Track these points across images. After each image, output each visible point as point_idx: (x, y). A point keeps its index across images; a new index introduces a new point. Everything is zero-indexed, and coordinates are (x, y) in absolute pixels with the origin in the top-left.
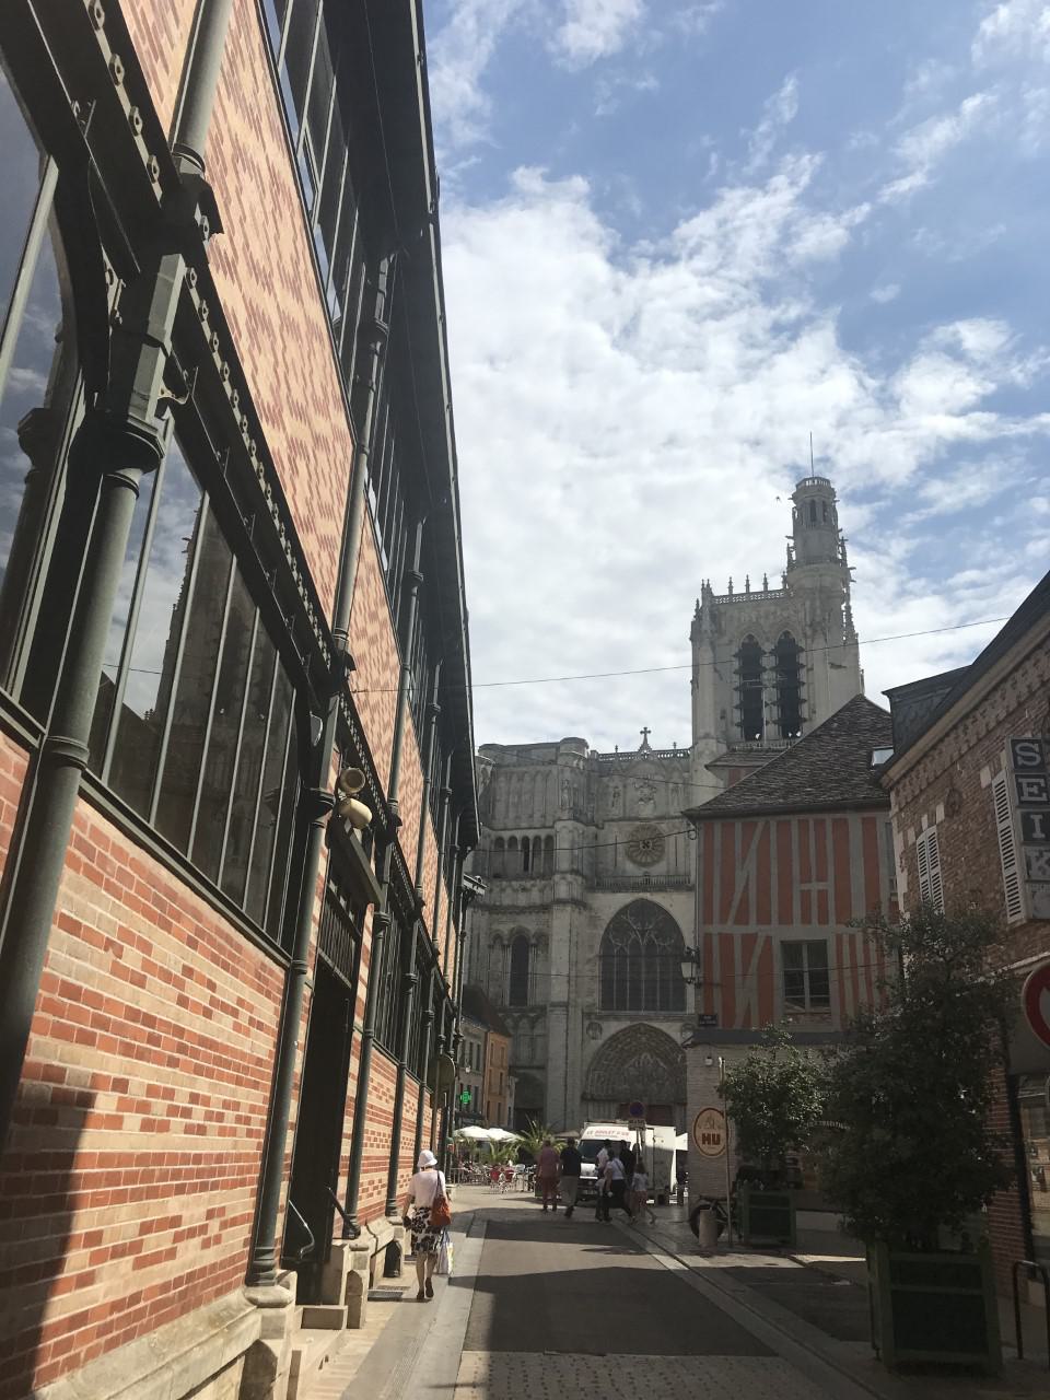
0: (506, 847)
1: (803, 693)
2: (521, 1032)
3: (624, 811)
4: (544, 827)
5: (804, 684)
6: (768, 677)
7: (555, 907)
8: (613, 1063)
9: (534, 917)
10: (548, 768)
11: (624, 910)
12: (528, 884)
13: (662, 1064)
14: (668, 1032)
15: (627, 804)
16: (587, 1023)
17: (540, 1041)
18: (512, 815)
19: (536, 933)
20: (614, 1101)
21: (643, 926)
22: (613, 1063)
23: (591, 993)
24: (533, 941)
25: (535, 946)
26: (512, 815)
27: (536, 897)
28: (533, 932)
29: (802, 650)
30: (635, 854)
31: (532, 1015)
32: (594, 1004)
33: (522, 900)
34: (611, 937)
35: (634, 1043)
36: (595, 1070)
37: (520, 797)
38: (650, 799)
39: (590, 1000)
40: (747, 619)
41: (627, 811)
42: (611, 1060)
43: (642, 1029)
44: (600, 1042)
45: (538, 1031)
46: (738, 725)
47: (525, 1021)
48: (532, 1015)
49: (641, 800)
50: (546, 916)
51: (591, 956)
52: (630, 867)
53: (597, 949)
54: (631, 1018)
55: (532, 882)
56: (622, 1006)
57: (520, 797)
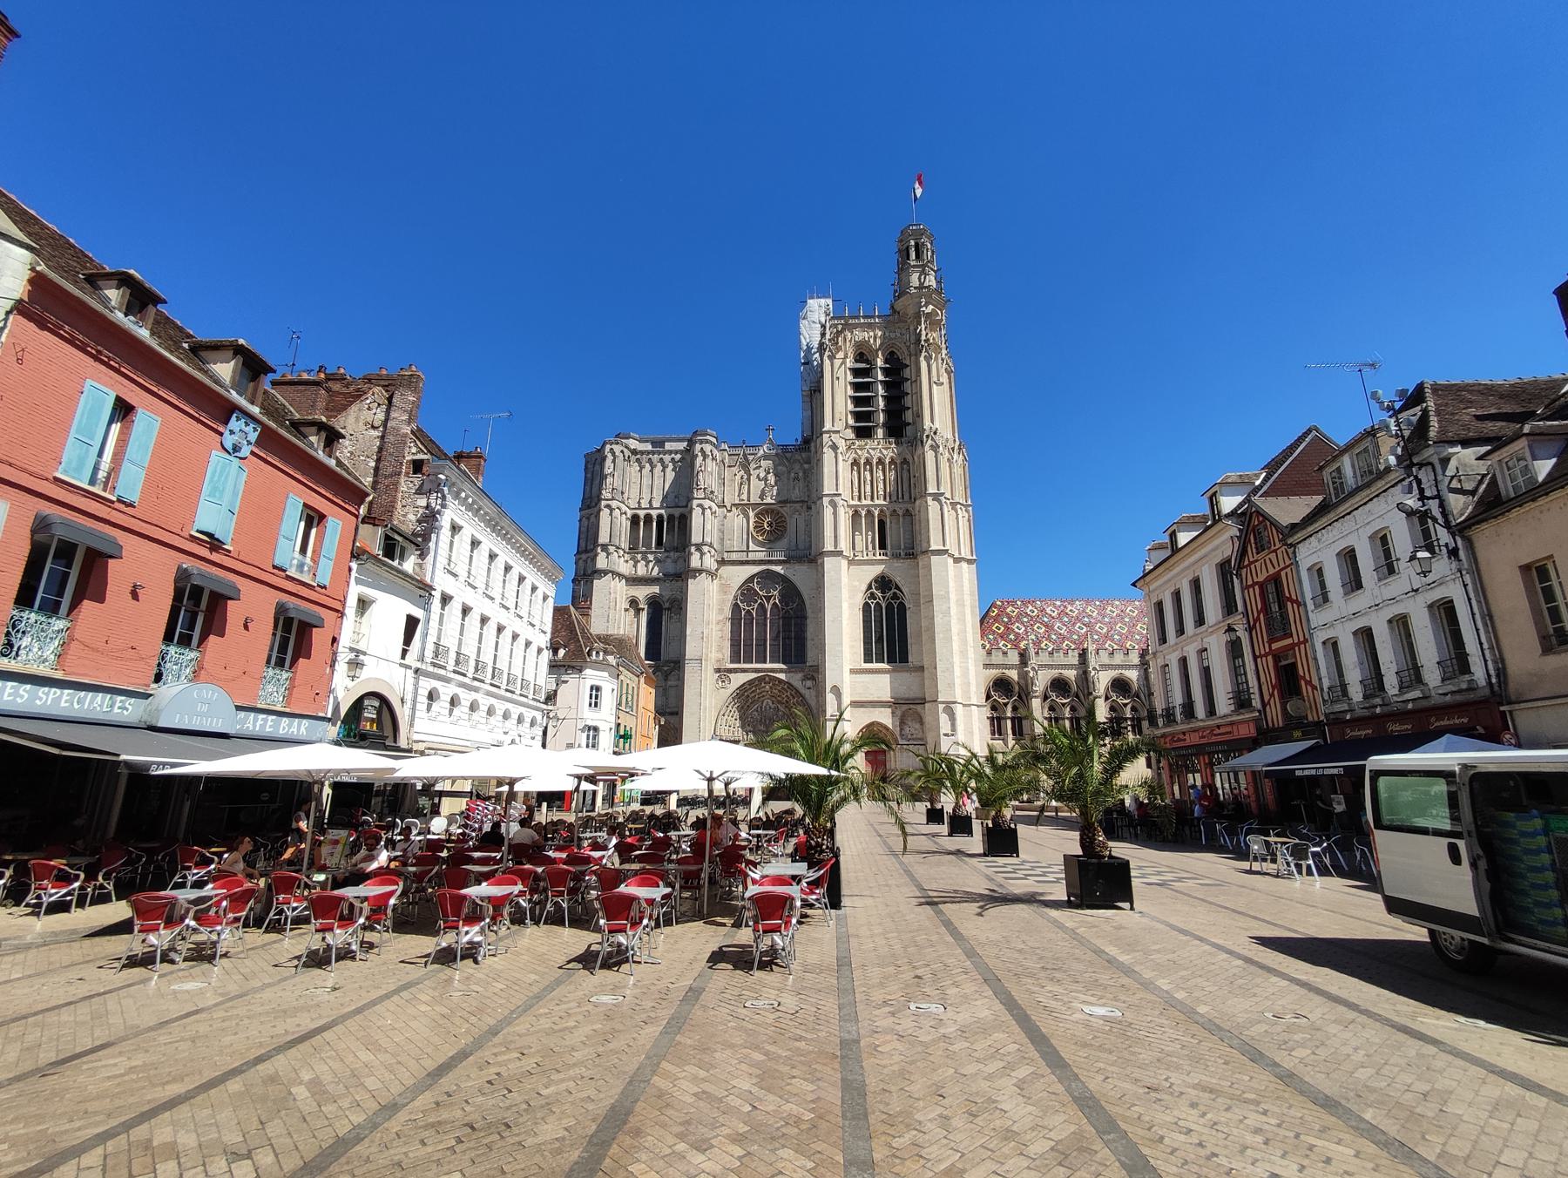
0: (642, 523)
1: (908, 401)
7: (691, 574)
11: (751, 579)
17: (672, 692)
23: (720, 649)
24: (667, 605)
25: (669, 609)
31: (666, 669)
39: (721, 656)
43: (767, 679)
44: (730, 691)
45: (669, 683)
48: (666, 669)
50: (680, 583)
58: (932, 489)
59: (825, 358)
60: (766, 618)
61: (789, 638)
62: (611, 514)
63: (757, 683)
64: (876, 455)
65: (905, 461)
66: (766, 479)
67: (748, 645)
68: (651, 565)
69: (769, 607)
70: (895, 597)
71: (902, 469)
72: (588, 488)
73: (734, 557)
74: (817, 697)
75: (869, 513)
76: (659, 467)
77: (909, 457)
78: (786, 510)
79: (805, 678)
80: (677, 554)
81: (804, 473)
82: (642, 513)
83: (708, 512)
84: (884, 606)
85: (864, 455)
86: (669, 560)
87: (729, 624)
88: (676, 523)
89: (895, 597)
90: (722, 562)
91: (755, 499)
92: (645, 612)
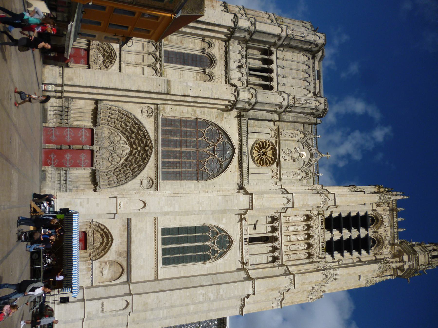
0: (266, 57)
2: (146, 56)
3: (285, 140)
4: (278, 84)
5: (351, 254)
6: (354, 233)
8: (123, 125)
9: (223, 73)
10: (312, 91)
12: (243, 70)
13: (122, 161)
15: (289, 142)
16: (153, 108)
17: (139, 70)
18: (284, 63)
19: (212, 73)
20: (95, 121)
21: (217, 151)
22: (123, 125)
24: (207, 71)
25: (204, 73)
26: (284, 63)
27: (235, 75)
28: (213, 71)
30: (258, 145)
32: (165, 113)
33: (233, 65)
34: (210, 127)
36: (119, 111)
37: (295, 70)
38: (291, 157)
40: (385, 220)
41: (284, 142)
42: (126, 125)
44: (139, 116)
45: (146, 68)
46: (331, 215)
48: (158, 66)
49: (291, 152)
52: (251, 142)
54: (156, 140)
55: (245, 73)
56: (165, 132)
57: (295, 70)
61: (181, 167)
67: (175, 133)
74: (134, 189)
75: (274, 229)
78: (274, 166)
81: (300, 180)
84: (208, 243)
86: (240, 75)
88: (266, 83)
89: (215, 252)
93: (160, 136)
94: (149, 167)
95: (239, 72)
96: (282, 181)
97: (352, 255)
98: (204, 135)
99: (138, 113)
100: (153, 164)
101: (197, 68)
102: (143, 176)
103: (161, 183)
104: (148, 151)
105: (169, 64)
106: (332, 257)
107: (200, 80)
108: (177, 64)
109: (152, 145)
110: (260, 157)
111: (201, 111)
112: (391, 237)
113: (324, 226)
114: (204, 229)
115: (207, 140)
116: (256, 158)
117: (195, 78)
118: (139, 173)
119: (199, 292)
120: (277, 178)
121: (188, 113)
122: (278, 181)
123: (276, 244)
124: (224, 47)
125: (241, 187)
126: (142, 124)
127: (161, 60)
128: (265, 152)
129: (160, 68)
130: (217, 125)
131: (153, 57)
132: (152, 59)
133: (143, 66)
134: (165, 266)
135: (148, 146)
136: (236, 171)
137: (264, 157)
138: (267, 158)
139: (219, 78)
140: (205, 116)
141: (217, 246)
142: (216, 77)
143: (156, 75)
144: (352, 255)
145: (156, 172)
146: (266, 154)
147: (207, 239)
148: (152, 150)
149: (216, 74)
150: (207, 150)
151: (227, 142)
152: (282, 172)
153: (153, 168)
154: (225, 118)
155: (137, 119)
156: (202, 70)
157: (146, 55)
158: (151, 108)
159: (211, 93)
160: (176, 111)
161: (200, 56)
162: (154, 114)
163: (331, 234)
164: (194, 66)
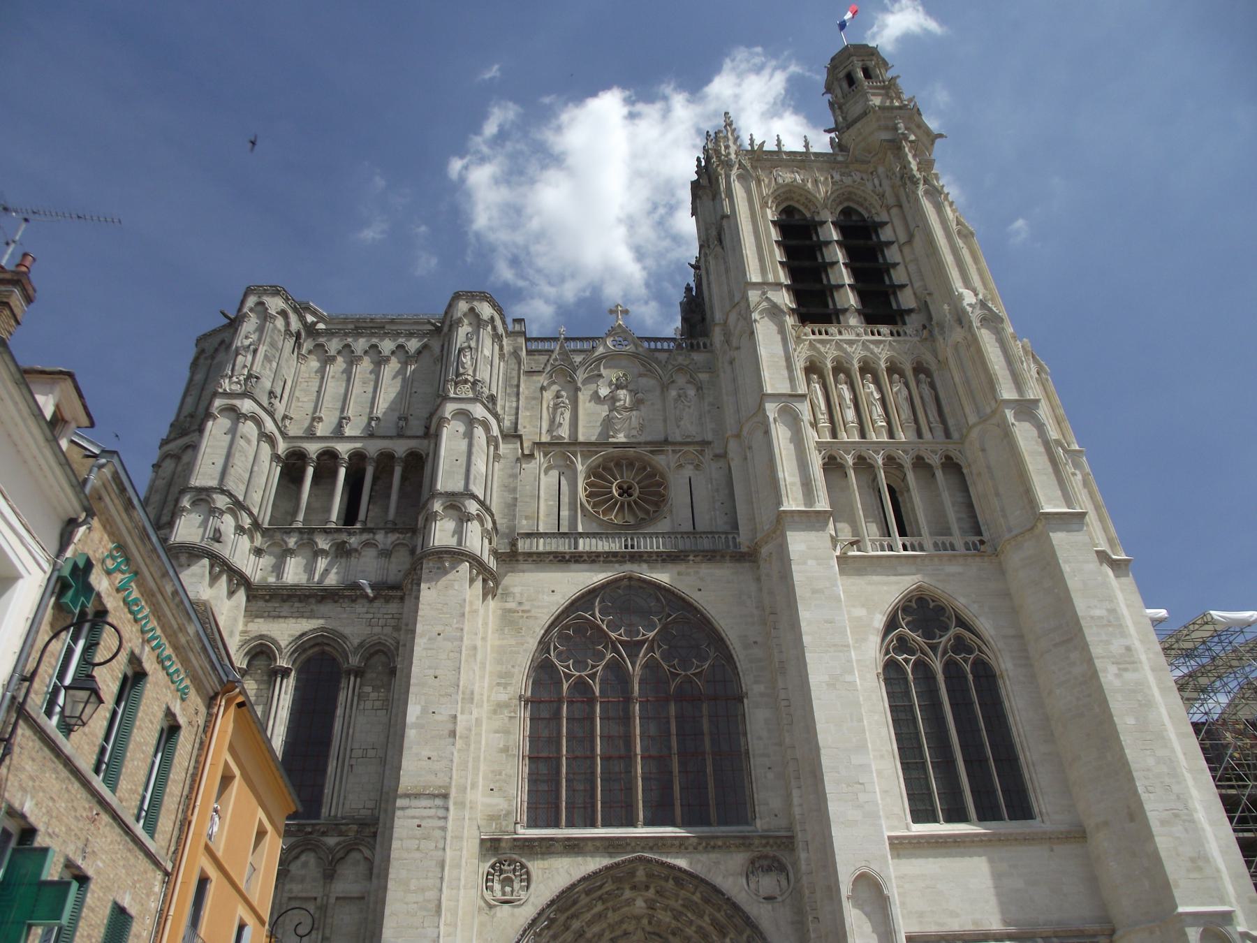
1: (898, 276)
4: (400, 435)
5: (895, 265)
11: (585, 599)
12: (354, 541)
14: (718, 881)
19: (361, 645)
24: (354, 661)
25: (359, 673)
28: (356, 642)
29: (886, 223)
32: (508, 814)
35: (612, 917)
39: (499, 803)
40: (788, 180)
43: (641, 874)
44: (527, 912)
47: (309, 858)
48: (331, 841)
50: (393, 608)
51: (503, 696)
53: (520, 682)
55: (365, 537)
58: (1007, 392)
59: (733, 177)
60: (628, 699)
62: (233, 431)
63: (607, 887)
64: (856, 356)
65: (919, 369)
66: (612, 399)
68: (322, 563)
69: (635, 669)
70: (960, 645)
71: (918, 382)
72: (189, 400)
73: (541, 545)
75: (863, 464)
76: (366, 365)
77: (928, 358)
79: (758, 866)
80: (392, 537)
82: (313, 448)
83: (479, 432)
84: (937, 666)
85: (829, 356)
86: (370, 554)
87: (524, 714)
89: (960, 645)
90: (511, 557)
91: (587, 432)
92: (289, 684)
93: (596, 831)
94: (709, 871)
95: (360, 554)
96: (709, 437)
97: (898, 264)
98: (580, 676)
99: (513, 915)
100: (698, 856)
101: (342, 697)
102: (744, 893)
103: (765, 827)
104: (650, 875)
105: (326, 799)
106: (913, 316)
107: (388, 687)
108: (324, 771)
109: (631, 861)
110: (635, 502)
111: (498, 684)
112: (833, 169)
113: (833, 329)
114: (892, 673)
115: (600, 668)
116: (641, 515)
117: (378, 704)
118: (735, 906)
119: (1117, 683)
120: (702, 452)
121: (507, 732)
122: (709, 453)
123: (907, 461)
124: (269, 604)
125: (747, 557)
126: (552, 902)
127: (309, 829)
128: (620, 487)
129: (341, 834)
130: (546, 631)
131: (297, 857)
132: (305, 865)
133: (332, 900)
134: (1036, 810)
135: (632, 874)
136: (697, 573)
137: (636, 494)
138: (638, 484)
139: (382, 622)
140: (516, 670)
141: (941, 637)
142: (377, 630)
143: (372, 848)
144: (898, 264)
145: (725, 846)
146: (625, 486)
147: (922, 668)
148: (649, 861)
149: (368, 631)
150: (633, 664)
151: (600, 603)
152: (679, 439)
153: (713, 856)
154: (520, 603)
155: (534, 921)
156: (352, 679)
157: (287, 887)
158: (493, 867)
159: (445, 639)
160: (500, 774)
161: (296, 688)
162: (514, 856)
163: (848, 314)
164: (335, 708)
